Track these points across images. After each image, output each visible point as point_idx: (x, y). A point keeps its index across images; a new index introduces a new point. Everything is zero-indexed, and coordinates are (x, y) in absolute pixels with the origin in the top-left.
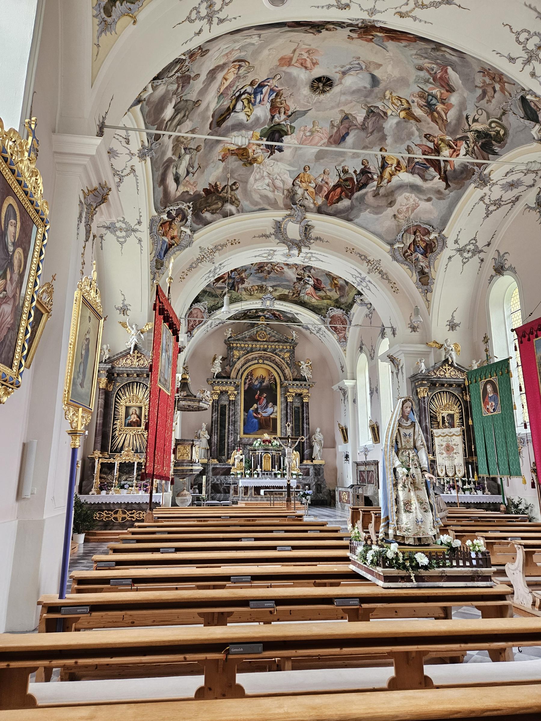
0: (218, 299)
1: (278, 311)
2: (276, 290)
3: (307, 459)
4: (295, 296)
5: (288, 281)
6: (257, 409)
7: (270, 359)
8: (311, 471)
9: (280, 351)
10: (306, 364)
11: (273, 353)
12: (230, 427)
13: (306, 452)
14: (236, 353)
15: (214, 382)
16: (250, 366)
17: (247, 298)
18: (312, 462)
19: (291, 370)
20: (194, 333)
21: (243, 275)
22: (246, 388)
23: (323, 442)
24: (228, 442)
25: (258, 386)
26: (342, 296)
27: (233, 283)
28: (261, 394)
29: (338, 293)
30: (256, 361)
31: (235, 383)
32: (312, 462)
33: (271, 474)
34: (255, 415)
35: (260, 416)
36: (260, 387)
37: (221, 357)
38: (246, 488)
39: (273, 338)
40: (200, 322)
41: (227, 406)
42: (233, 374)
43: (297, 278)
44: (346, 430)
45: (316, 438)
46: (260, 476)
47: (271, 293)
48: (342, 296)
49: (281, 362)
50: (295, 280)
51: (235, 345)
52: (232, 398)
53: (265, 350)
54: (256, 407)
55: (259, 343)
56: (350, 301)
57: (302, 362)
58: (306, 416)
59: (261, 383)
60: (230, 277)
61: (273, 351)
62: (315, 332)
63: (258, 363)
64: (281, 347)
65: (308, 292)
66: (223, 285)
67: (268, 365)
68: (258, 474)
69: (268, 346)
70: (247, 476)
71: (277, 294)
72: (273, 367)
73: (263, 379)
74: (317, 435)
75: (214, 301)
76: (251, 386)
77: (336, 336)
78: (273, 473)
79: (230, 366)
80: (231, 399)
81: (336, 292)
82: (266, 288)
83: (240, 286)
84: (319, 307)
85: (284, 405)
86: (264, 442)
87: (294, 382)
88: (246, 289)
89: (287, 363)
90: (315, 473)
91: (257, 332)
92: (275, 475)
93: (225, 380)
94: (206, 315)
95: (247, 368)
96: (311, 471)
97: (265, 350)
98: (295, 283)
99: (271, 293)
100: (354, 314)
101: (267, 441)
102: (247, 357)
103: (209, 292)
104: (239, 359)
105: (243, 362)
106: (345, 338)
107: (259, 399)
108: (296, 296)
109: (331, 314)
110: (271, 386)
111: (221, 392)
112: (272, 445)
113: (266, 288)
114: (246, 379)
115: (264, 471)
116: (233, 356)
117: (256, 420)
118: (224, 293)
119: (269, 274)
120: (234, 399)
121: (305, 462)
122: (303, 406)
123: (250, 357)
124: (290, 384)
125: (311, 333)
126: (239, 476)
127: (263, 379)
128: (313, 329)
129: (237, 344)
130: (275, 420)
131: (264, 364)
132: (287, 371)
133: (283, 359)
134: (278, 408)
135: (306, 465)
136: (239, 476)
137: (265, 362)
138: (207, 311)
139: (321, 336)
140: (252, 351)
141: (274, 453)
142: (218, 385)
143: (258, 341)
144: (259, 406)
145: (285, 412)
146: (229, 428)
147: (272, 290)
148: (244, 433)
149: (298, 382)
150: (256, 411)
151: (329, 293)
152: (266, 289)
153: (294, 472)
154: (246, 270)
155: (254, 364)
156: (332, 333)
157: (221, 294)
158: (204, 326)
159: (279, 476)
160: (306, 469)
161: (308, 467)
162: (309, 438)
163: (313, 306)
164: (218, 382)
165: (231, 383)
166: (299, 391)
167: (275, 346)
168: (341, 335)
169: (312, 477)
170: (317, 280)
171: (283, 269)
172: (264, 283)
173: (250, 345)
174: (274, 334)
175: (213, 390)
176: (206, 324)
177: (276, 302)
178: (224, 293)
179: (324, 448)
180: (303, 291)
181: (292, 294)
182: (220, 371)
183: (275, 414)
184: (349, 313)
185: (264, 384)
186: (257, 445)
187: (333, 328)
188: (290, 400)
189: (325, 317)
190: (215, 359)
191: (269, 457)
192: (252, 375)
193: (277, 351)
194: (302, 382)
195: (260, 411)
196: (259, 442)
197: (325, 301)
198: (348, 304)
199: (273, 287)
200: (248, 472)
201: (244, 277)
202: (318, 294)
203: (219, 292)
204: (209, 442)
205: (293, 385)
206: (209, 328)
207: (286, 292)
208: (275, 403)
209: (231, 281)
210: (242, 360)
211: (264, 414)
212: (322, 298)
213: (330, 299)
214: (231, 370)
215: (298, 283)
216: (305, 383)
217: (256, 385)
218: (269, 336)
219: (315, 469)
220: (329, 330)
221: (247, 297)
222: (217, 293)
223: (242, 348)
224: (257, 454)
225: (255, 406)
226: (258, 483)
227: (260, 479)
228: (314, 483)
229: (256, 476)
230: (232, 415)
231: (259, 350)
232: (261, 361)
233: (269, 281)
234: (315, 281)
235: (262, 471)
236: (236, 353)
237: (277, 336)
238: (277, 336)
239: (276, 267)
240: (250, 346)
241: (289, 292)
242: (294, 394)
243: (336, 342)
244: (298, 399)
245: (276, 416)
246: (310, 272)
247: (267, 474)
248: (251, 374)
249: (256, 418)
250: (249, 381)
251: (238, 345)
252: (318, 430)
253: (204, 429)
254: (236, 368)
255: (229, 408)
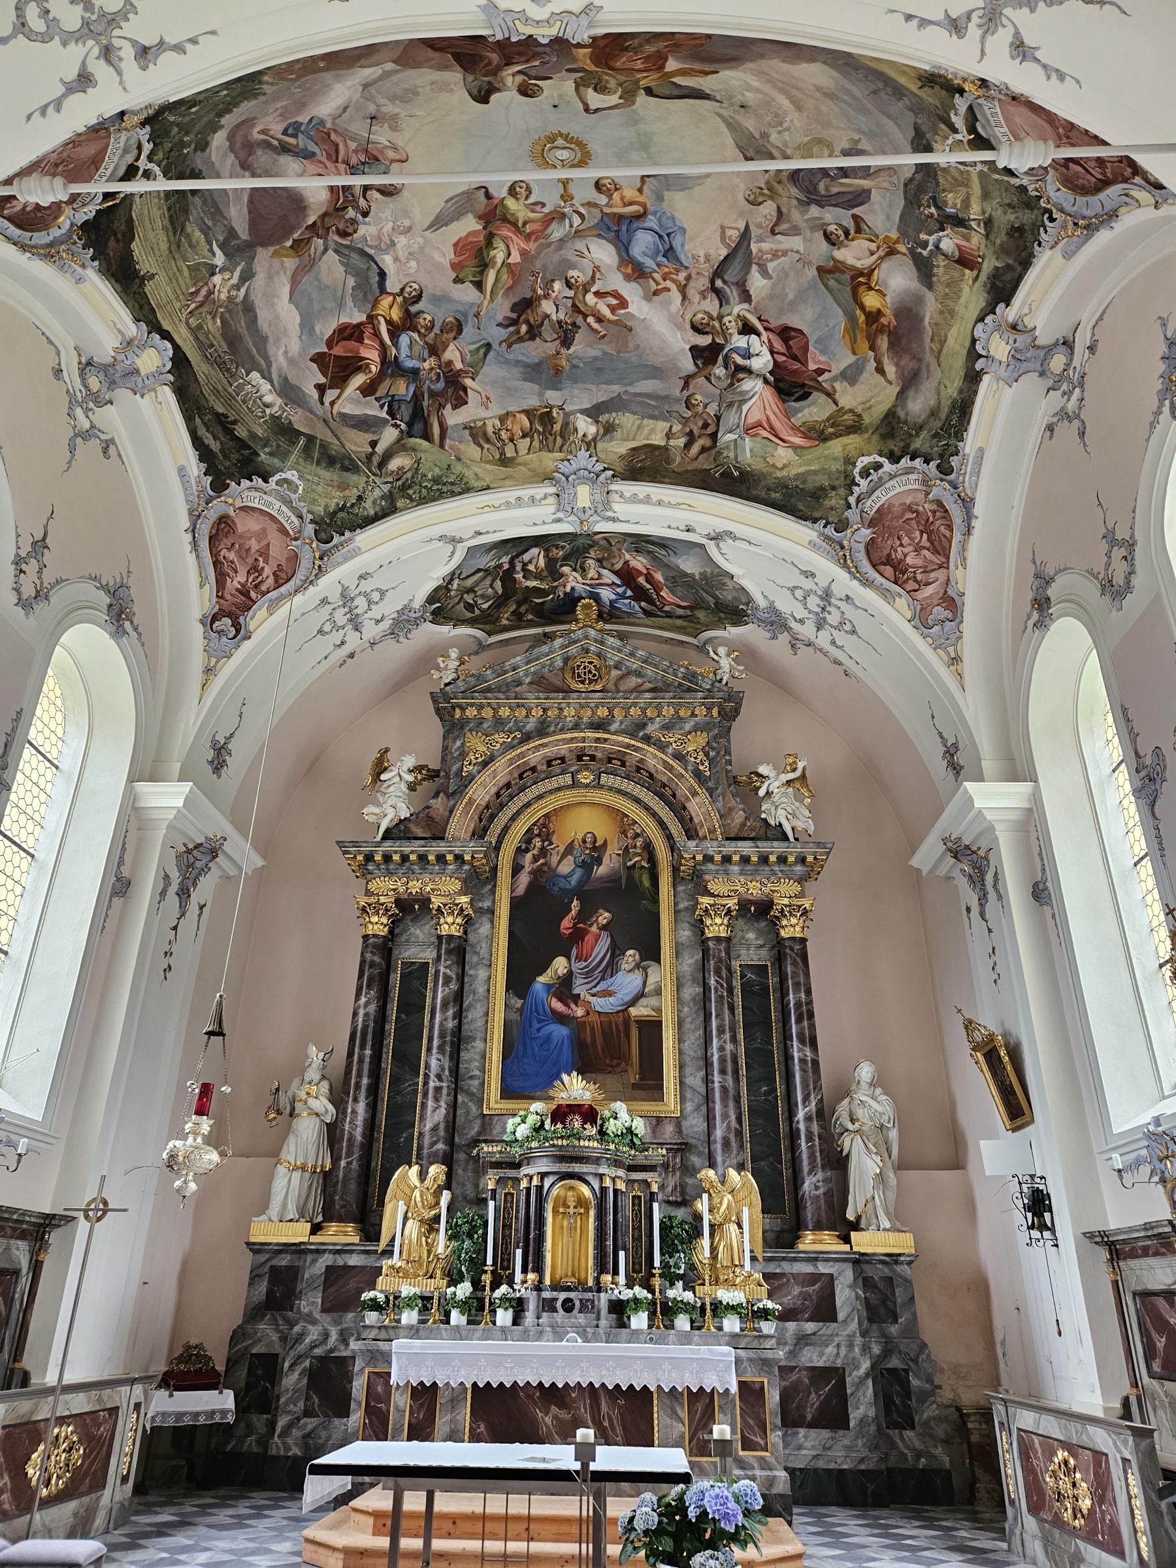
0: (359, 480)
1: (640, 543)
2: (609, 429)
3: (818, 1227)
4: (695, 448)
5: (656, 372)
6: (567, 980)
7: (615, 761)
8: (845, 1296)
9: (667, 727)
10: (785, 777)
11: (633, 735)
12: (434, 1063)
13: (812, 1184)
14: (477, 745)
15: (369, 858)
16: (540, 797)
17: (488, 480)
18: (847, 1240)
19: (714, 801)
20: (251, 628)
21: (452, 354)
22: (521, 890)
23: (893, 1134)
24: (421, 1134)
25: (574, 880)
26: (909, 382)
27: (417, 398)
28: (585, 915)
29: (890, 369)
30: (568, 779)
31: (459, 858)
32: (847, 1240)
33: (587, 1307)
34: (557, 1005)
35: (580, 1012)
36: (582, 882)
37: (410, 761)
38: (425, 1394)
39: (633, 681)
40: (281, 578)
41: (432, 970)
42: (460, 825)
43: (694, 350)
44: (1015, 1054)
45: (860, 1113)
46: (529, 1316)
47: (590, 444)
48: (909, 382)
49: (670, 768)
50: (687, 365)
51: (471, 712)
52: (450, 926)
53: (600, 725)
54: (562, 971)
55: (574, 700)
56: (952, 389)
57: (763, 770)
58: (798, 1005)
59: (587, 866)
60: (391, 367)
61: (636, 729)
62: (807, 631)
63: (575, 784)
64: (668, 712)
65: (752, 420)
66: (373, 409)
67: (620, 792)
68: (518, 1307)
69: (611, 711)
70: (456, 1317)
71: (618, 447)
72: (637, 801)
73: (597, 851)
74: (862, 1095)
75: (343, 487)
76: (541, 883)
77: (902, 602)
78: (604, 1298)
79: (449, 796)
80: (445, 930)
81: (880, 370)
82: (566, 424)
83: (454, 417)
84: (810, 485)
85: (690, 960)
86: (560, 1114)
87: (729, 848)
88: (477, 433)
89: (698, 774)
90: (867, 1303)
91: (566, 660)
92: (619, 1309)
93: (412, 848)
94: (307, 553)
95: (528, 805)
96: (845, 1296)
97: (600, 725)
98: (687, 380)
99: (590, 444)
100: (981, 452)
101: (574, 1109)
102: (522, 755)
103: (311, 439)
104: (485, 764)
105: (502, 778)
106: (951, 603)
107: (578, 935)
108: (704, 450)
109: (872, 505)
110: (630, 878)
111: (398, 902)
112: (602, 1133)
113: (566, 424)
114: (520, 851)
115: (555, 1287)
116: (463, 755)
117: (560, 1032)
118: (380, 449)
119: (567, 342)
120: (455, 931)
121: (809, 1242)
122: (779, 959)
123: (535, 758)
124: (708, 859)
125: (795, 643)
126: (409, 1317)
127: (597, 851)
128: (800, 613)
129: (481, 707)
130: (653, 1028)
131: (599, 786)
132: (699, 807)
133: (679, 756)
134: (661, 975)
135: (814, 1258)
136: (409, 1317)
137: (604, 778)
138: (310, 529)
139: (841, 639)
140: (542, 730)
141: (614, 1178)
142: (390, 873)
143: (568, 691)
144: (577, 966)
145: (699, 990)
146: (427, 1066)
147: (592, 430)
148: (507, 1093)
149: (746, 848)
150: (564, 988)
151: (848, 397)
152: (568, 429)
153: (727, 1296)
154: (459, 328)
155: (559, 789)
156: (886, 594)
157: (369, 457)
158: (299, 599)
159: (639, 1321)
160: (814, 1278)
161: (824, 1268)
162: (823, 1114)
163: (782, 485)
164: (387, 858)
165: (441, 858)
166: (755, 890)
167: (644, 710)
168: (929, 591)
169: (854, 1326)
170: (786, 333)
171: (623, 304)
172: (553, 397)
173: (535, 706)
174: (635, 664)
175: (368, 893)
176: (313, 594)
177: (618, 486)
178: (380, 449)
179: (902, 1166)
180: (730, 418)
181: (682, 441)
182: (404, 813)
183: (653, 1001)
184: (955, 461)
185: (601, 870)
186: (523, 1131)
187: (888, 571)
188: (717, 927)
189: (842, 526)
190: (380, 767)
191: (581, 1202)
192: (547, 837)
193: (651, 729)
194: (765, 847)
195: (580, 988)
196: (532, 1119)
197: (836, 447)
198: (945, 411)
199: (593, 413)
200: (464, 1289)
201: (458, 365)
202: (798, 420)
203: (356, 443)
204: (333, 1133)
205: (727, 859)
206: (354, 640)
207: (655, 433)
208: (651, 953)
209: (402, 389)
210: (501, 770)
211: (601, 1004)
212: (818, 434)
213: (855, 428)
214: (451, 812)
215: (701, 380)
216: (777, 847)
217: (566, 877)
218: (615, 673)
219: (867, 1283)
220: (866, 583)
221: (489, 472)
222: (350, 447)
223: (499, 723)
224: (524, 1184)
225: (560, 965)
226: (497, 1360)
227: (525, 1336)
228: (866, 1365)
229: (504, 1317)
230: (445, 1005)
231: (576, 727)
232: (586, 777)
233: (575, 381)
234: (779, 345)
235: (538, 1288)
236: (477, 745)
237: (649, 671)
238: (649, 671)
239: (590, 298)
240: (537, 713)
241: (669, 435)
242: (732, 903)
243: (908, 629)
244: (760, 933)
245: (659, 1010)
246: (746, 297)
247: (568, 1306)
248: (543, 830)
249: (561, 1019)
250: (535, 859)
251: (487, 713)
252: (865, 1072)
253: (313, 1074)
254: (471, 802)
255: (437, 972)
